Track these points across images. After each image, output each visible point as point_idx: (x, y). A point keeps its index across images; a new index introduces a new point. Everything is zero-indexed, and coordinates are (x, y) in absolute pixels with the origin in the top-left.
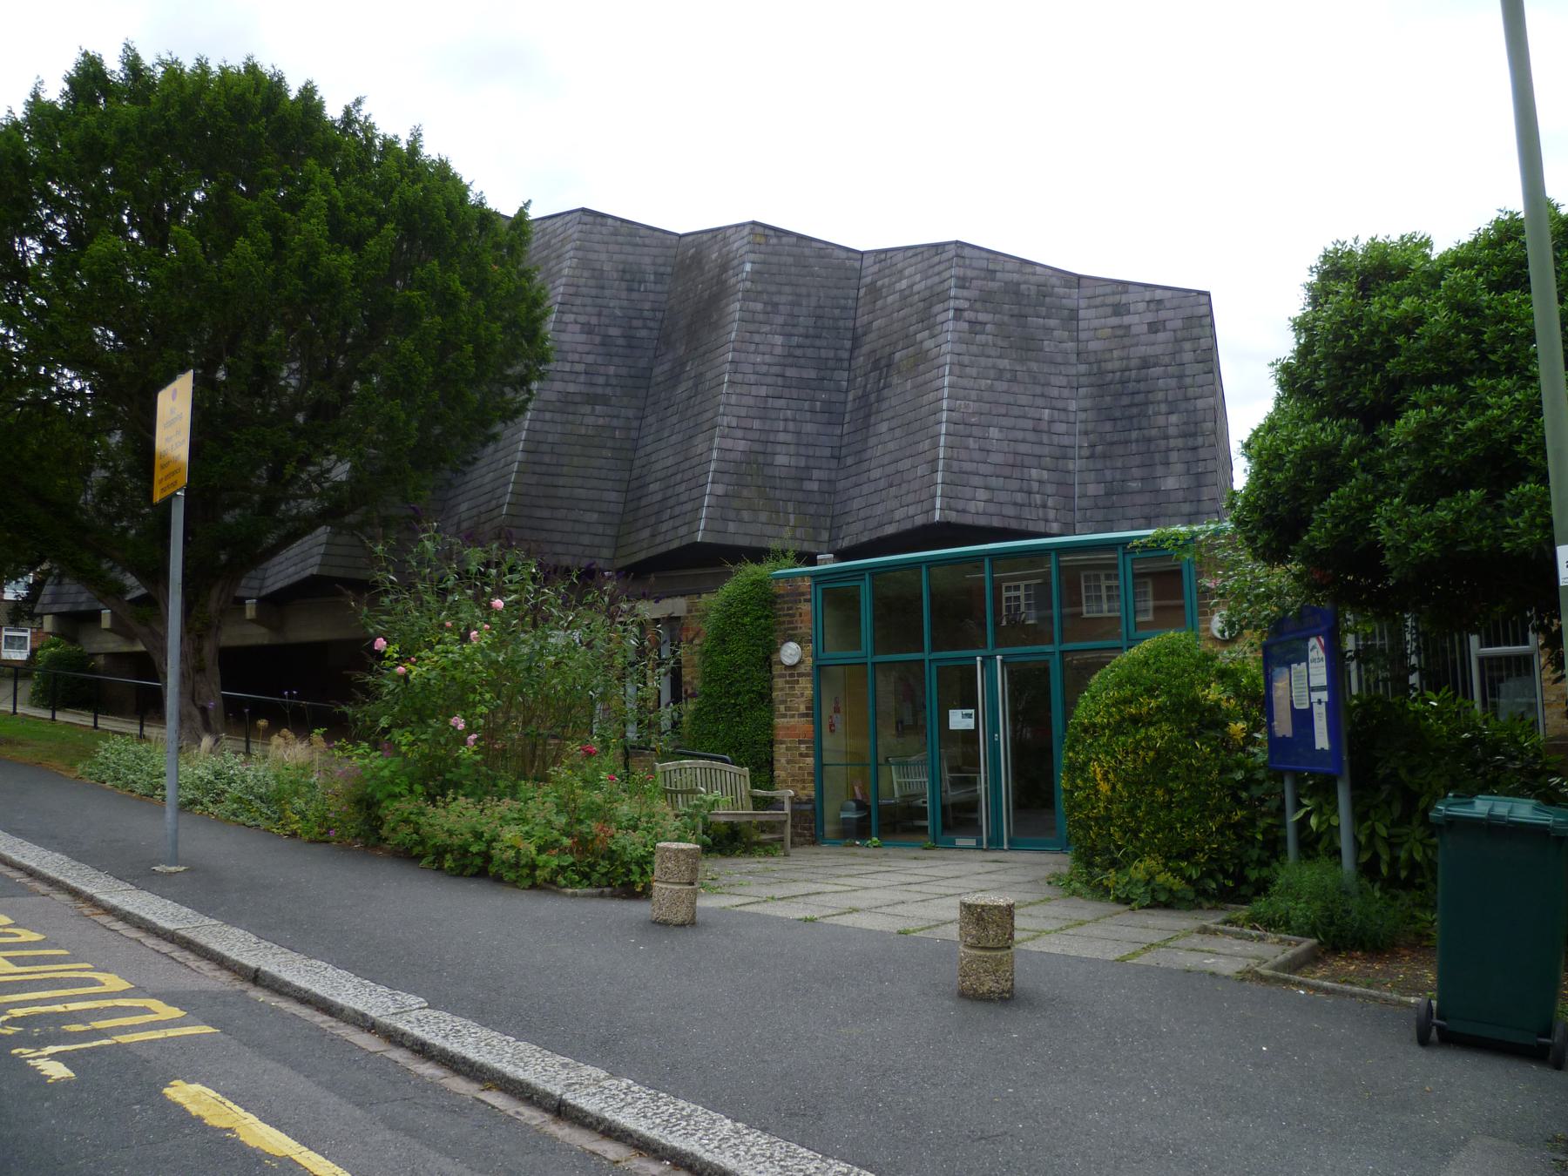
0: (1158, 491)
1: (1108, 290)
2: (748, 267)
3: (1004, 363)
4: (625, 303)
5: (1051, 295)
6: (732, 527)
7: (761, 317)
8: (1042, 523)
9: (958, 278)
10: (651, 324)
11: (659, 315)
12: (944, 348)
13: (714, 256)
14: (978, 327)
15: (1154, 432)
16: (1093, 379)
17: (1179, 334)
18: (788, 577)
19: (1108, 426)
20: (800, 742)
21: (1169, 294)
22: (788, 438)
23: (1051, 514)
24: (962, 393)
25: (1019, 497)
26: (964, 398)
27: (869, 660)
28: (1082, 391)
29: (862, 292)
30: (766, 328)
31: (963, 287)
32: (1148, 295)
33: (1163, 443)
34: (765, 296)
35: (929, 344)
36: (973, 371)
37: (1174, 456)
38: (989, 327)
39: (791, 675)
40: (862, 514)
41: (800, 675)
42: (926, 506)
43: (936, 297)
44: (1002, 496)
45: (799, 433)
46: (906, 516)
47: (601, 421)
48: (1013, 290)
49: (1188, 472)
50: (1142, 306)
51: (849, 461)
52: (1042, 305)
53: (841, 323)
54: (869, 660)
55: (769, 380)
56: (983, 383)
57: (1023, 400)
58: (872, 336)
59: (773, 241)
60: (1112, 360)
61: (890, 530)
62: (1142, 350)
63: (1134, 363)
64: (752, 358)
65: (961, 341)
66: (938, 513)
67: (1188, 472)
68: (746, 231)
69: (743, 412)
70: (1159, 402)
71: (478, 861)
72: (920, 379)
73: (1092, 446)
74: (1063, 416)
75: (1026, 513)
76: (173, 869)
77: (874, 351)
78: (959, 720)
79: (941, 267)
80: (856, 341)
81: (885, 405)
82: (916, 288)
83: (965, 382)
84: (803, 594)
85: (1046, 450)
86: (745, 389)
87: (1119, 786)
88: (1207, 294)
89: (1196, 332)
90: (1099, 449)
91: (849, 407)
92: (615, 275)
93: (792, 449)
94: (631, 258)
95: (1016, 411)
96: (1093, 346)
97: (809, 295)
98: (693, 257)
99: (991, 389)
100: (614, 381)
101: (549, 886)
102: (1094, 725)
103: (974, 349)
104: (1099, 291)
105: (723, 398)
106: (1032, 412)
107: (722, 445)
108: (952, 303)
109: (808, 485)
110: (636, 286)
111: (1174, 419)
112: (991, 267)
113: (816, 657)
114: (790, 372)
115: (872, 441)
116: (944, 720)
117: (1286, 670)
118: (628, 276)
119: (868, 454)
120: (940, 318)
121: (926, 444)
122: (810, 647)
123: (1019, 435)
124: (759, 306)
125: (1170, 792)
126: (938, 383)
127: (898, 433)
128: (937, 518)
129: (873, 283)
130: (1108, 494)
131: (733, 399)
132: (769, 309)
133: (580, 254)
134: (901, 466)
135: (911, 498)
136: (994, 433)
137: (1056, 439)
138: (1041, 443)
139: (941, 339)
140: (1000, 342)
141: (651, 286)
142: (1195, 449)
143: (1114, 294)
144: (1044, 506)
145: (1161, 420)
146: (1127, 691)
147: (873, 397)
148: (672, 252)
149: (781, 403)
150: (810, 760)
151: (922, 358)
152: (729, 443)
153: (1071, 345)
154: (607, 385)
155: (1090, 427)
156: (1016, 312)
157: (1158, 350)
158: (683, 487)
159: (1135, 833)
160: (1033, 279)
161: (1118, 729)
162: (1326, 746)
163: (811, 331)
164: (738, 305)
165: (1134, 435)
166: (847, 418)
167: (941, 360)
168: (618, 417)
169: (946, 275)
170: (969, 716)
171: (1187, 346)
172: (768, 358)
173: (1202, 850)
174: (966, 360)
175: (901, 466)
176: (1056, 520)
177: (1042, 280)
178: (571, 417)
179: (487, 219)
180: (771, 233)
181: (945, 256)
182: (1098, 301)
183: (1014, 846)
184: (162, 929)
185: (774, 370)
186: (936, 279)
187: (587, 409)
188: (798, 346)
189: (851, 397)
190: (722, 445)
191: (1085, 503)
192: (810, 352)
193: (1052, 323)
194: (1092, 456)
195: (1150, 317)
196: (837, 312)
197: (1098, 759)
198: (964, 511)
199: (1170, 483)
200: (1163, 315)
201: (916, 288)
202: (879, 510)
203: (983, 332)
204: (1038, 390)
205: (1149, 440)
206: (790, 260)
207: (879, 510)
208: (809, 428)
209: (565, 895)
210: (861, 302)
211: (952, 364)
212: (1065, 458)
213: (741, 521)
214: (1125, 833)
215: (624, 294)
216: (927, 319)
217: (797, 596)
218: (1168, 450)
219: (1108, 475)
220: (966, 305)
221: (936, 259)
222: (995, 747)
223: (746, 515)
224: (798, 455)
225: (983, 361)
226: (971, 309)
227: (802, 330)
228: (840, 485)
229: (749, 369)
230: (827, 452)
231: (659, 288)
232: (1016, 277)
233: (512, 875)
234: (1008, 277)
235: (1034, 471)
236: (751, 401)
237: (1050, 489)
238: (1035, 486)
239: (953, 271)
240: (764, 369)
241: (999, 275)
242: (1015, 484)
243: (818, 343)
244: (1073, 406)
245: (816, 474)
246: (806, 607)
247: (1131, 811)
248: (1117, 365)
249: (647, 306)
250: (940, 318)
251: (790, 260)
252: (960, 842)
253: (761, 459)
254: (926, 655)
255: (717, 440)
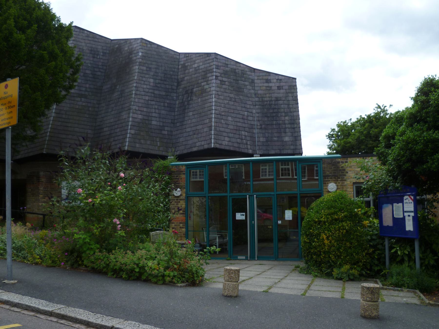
0: (283, 141)
1: (264, 74)
2: (140, 54)
3: (232, 95)
4: (92, 62)
5: (246, 74)
6: (137, 145)
7: (145, 72)
8: (246, 150)
9: (216, 65)
10: (101, 70)
11: (105, 67)
12: (212, 89)
13: (126, 49)
14: (223, 83)
15: (281, 122)
16: (260, 103)
17: (287, 91)
18: (176, 165)
19: (266, 119)
20: (180, 223)
21: (283, 77)
22: (156, 115)
23: (249, 147)
24: (219, 104)
25: (239, 141)
26: (220, 106)
27: (207, 195)
28: (257, 107)
29: (180, 67)
30: (147, 76)
31: (218, 69)
32: (277, 77)
33: (284, 126)
34: (147, 65)
35: (206, 87)
36: (222, 97)
37: (287, 130)
38: (227, 83)
39: (177, 200)
40: (184, 143)
41: (180, 200)
42: (208, 142)
43: (208, 71)
44: (234, 140)
45: (160, 114)
46: (199, 145)
47: (84, 104)
48: (234, 71)
49: (292, 136)
50: (275, 81)
51: (178, 124)
52: (243, 77)
53: (173, 77)
54: (207, 195)
55: (149, 94)
56: (226, 102)
57: (239, 108)
58: (185, 82)
59: (149, 46)
60: (266, 97)
61: (195, 149)
62: (276, 95)
63: (273, 99)
64: (143, 86)
65: (218, 87)
66: (213, 145)
67: (292, 136)
68: (139, 41)
69: (140, 105)
70: (282, 112)
71: (137, 274)
72: (204, 99)
73: (261, 125)
74: (251, 115)
75: (241, 146)
76: (12, 282)
77: (186, 87)
78: (239, 216)
79: (210, 61)
80: (179, 84)
81: (191, 106)
82: (200, 67)
83: (220, 101)
84: (182, 172)
85: (246, 126)
86: (140, 97)
87: (333, 241)
88: (295, 79)
89: (293, 91)
90: (263, 126)
91: (177, 106)
92: (88, 51)
93: (158, 119)
94: (94, 46)
95: (236, 112)
96: (260, 92)
97: (162, 66)
98: (117, 48)
99: (228, 104)
100: (89, 90)
101: (171, 283)
102: (321, 221)
103: (222, 90)
104: (261, 74)
105: (133, 100)
106: (241, 113)
107: (133, 117)
108: (214, 74)
109: (164, 132)
110: (96, 56)
111: (287, 118)
112: (226, 63)
113: (186, 193)
114: (156, 92)
115: (186, 118)
116: (234, 216)
117: (390, 206)
118: (93, 52)
119: (185, 123)
120: (210, 78)
121: (207, 121)
122: (185, 190)
123: (238, 120)
124: (145, 68)
125: (351, 243)
126: (210, 100)
127: (196, 116)
128: (213, 146)
129: (184, 64)
130: (267, 141)
131: (137, 100)
132: (148, 69)
133: (75, 42)
134: (199, 127)
135: (202, 139)
136: (230, 118)
137: (249, 122)
138: (245, 123)
139: (211, 85)
140: (230, 88)
141: (101, 57)
142: (294, 128)
143: (266, 76)
144: (247, 144)
145: (283, 118)
146: (332, 210)
147: (186, 103)
148: (109, 45)
149: (153, 103)
150: (184, 230)
151: (204, 91)
152: (135, 116)
153: (253, 91)
154: (86, 91)
155: (260, 119)
156: (235, 79)
157: (281, 95)
158: (118, 130)
159: (339, 257)
160: (240, 68)
161: (331, 223)
162: (412, 229)
163: (163, 78)
164: (137, 67)
165: (274, 122)
166: (176, 110)
167: (211, 93)
168: (90, 103)
169: (212, 64)
170: (243, 215)
171: (290, 95)
172: (148, 87)
173: (361, 262)
174: (220, 93)
175: (199, 127)
176: (251, 149)
177: (243, 69)
178: (72, 102)
179: (61, 26)
180: (148, 43)
181: (211, 57)
182: (261, 77)
183: (259, 259)
184: (43, 310)
185: (150, 91)
186: (208, 65)
187: (79, 99)
188: (159, 83)
189: (177, 102)
190: (133, 117)
191: (260, 144)
192: (163, 86)
193: (247, 83)
194: (261, 128)
195: (278, 84)
196: (171, 73)
197: (324, 232)
198: (221, 144)
199: (287, 139)
200: (282, 84)
201: (200, 67)
202: (190, 142)
203: (225, 85)
204: (243, 105)
205: (280, 124)
206: (155, 53)
207: (190, 142)
208: (163, 112)
209: (178, 286)
210: (180, 70)
211: (215, 94)
212: (252, 128)
213: (141, 143)
214: (335, 257)
215: (91, 59)
216: (205, 78)
217: (180, 172)
218: (285, 128)
219: (267, 135)
220: (219, 75)
221: (208, 58)
222: (252, 226)
223: (142, 141)
224: (160, 121)
225: (225, 94)
226: (221, 76)
227: (160, 78)
228: (174, 133)
229: (142, 90)
230: (170, 121)
231: (104, 58)
232: (234, 67)
233: (154, 280)
234: (232, 67)
235: (243, 132)
236: (142, 101)
237: (248, 138)
238: (244, 137)
239: (214, 63)
240: (147, 90)
241: (229, 66)
242: (237, 136)
243: (165, 83)
244: (254, 111)
245: (166, 128)
246: (183, 176)
247: (338, 250)
248: (268, 99)
249: (100, 64)
250: (210, 78)
251: (155, 53)
252: (239, 257)
253: (147, 122)
254: (228, 194)
255: (131, 114)
